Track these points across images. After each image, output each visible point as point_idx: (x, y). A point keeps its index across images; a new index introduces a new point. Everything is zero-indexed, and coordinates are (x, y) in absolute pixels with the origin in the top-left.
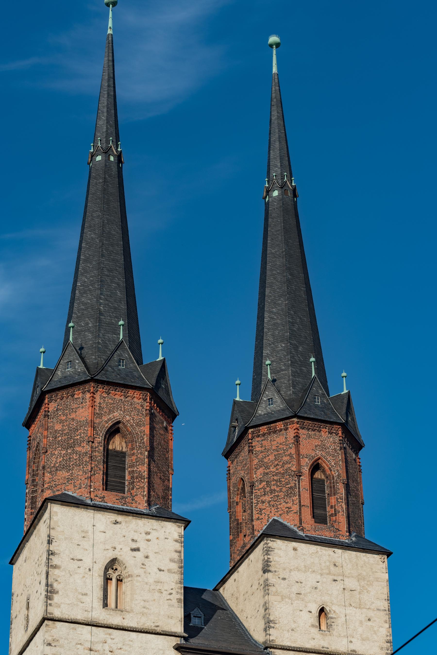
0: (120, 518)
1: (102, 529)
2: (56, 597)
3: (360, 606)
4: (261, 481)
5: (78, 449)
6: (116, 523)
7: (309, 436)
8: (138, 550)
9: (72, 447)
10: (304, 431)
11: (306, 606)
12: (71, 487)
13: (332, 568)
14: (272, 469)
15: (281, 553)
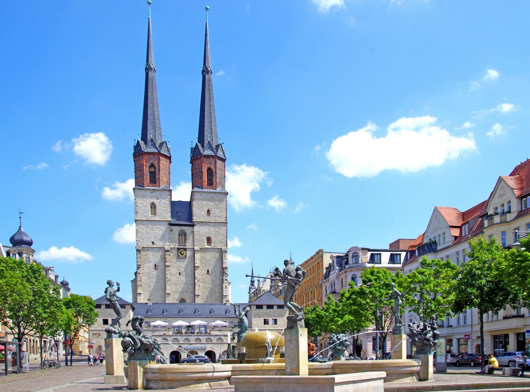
0: (153, 191)
1: (149, 194)
2: (138, 214)
3: (219, 208)
4: (195, 174)
5: (142, 172)
6: (152, 192)
7: (207, 160)
8: (158, 199)
9: (140, 171)
10: (205, 159)
11: (203, 210)
12: (141, 183)
13: (211, 198)
14: (197, 170)
15: (197, 196)
